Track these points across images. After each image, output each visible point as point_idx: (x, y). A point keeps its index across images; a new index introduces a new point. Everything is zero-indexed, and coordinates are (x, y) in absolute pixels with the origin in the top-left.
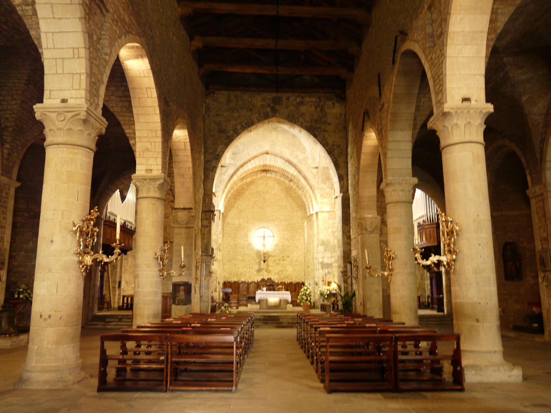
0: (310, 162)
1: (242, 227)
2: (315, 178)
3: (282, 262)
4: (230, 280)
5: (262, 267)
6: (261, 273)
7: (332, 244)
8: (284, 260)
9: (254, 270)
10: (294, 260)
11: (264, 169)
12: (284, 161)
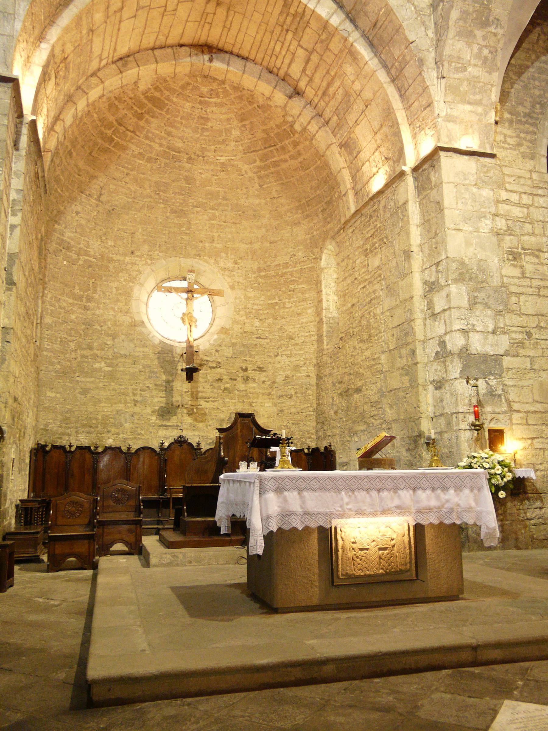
1: (111, 266)
2: (423, 23)
3: (241, 386)
4: (64, 442)
5: (177, 399)
6: (174, 421)
7: (496, 281)
8: (246, 379)
9: (149, 410)
10: (280, 379)
11: (203, 40)
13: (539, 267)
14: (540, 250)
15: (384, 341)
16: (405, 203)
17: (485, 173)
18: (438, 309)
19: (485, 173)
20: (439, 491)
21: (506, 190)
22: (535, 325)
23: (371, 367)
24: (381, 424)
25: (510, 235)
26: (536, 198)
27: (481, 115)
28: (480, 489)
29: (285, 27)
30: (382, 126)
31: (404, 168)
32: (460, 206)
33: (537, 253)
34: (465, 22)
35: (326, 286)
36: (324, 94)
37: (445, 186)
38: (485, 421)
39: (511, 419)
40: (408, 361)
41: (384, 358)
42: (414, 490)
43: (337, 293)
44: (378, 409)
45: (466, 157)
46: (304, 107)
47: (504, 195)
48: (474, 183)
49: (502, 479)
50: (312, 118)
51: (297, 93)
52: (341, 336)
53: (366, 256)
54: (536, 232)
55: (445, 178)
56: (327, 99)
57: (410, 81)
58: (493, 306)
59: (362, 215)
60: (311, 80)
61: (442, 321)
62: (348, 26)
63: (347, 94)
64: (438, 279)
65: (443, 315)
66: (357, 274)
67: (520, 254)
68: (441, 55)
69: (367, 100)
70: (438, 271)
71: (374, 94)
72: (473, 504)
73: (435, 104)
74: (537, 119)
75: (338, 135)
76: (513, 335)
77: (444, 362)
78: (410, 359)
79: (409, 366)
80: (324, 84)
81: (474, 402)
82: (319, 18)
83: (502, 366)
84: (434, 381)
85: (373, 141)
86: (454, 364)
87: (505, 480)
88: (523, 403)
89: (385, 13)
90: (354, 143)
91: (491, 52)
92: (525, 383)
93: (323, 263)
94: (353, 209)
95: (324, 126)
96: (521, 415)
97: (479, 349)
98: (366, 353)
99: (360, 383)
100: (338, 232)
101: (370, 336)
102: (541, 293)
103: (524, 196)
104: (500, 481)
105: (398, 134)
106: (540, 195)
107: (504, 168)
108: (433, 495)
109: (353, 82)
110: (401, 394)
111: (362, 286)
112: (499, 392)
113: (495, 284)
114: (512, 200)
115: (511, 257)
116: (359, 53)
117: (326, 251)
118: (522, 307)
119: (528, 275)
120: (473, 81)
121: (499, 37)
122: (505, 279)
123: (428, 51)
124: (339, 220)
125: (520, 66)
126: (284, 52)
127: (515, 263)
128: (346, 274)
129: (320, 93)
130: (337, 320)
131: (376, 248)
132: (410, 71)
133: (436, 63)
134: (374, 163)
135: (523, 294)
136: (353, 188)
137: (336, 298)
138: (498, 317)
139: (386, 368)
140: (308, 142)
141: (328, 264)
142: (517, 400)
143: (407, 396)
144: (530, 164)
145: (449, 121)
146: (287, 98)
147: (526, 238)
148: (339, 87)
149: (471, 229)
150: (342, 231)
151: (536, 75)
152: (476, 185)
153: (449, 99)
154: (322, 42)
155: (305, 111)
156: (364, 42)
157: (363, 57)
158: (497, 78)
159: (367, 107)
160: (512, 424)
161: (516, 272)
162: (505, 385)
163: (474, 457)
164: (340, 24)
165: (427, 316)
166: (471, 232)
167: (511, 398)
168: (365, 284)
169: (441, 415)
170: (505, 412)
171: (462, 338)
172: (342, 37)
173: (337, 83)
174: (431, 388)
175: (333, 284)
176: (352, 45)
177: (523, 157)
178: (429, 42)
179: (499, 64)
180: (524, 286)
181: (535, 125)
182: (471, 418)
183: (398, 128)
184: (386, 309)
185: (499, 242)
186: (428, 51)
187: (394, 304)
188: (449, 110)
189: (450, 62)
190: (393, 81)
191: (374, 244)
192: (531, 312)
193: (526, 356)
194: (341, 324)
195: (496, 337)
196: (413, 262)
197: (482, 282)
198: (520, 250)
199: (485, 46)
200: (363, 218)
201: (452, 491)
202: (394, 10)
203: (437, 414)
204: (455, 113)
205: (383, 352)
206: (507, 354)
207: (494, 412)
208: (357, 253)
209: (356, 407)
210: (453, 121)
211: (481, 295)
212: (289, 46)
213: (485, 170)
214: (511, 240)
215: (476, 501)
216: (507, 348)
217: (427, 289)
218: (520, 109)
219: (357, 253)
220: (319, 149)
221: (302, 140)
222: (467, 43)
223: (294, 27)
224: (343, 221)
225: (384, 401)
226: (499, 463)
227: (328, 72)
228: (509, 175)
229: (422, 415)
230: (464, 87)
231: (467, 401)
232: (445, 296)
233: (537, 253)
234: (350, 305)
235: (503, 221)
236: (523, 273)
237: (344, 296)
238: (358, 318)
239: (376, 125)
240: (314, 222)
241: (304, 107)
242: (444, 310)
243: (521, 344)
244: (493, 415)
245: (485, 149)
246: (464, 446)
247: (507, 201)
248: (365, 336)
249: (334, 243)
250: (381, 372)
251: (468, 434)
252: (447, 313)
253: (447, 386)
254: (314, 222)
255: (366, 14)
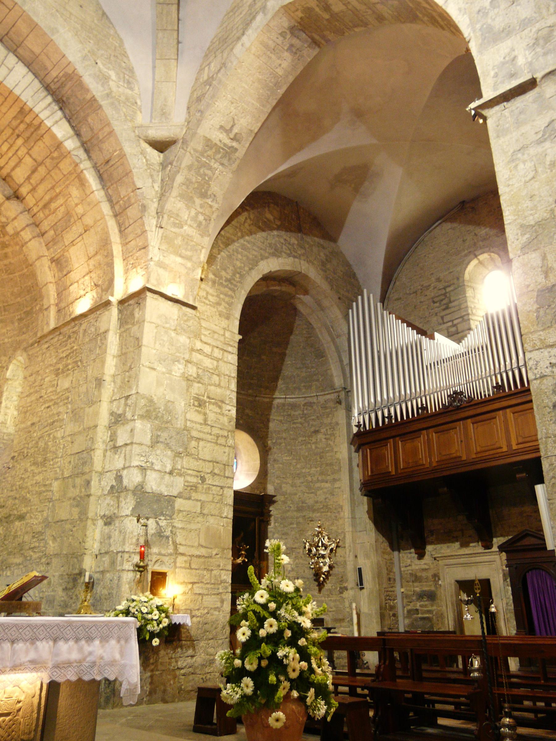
0: (141, 119)
7: (180, 424)
12: (37, 84)
13: (220, 417)
14: (222, 402)
15: (59, 467)
16: (106, 332)
17: (185, 321)
18: (120, 443)
19: (185, 321)
20: (83, 642)
21: (201, 340)
22: (209, 471)
23: (40, 493)
24: (40, 558)
25: (199, 382)
26: (225, 354)
27: (189, 269)
28: (127, 640)
29: (17, 132)
30: (96, 253)
31: (111, 298)
32: (157, 346)
33: (220, 404)
34: (188, 188)
35: (7, 398)
36: (45, 206)
37: (146, 324)
38: (150, 563)
39: (175, 562)
40: (81, 492)
41: (56, 485)
42: (55, 640)
43: (18, 409)
44: (39, 541)
45: (170, 303)
46: (21, 213)
47: (199, 345)
48: (173, 328)
49: (158, 625)
50: (27, 226)
51: (17, 196)
52: (13, 454)
53: (57, 375)
54: (222, 384)
55: (148, 317)
56: (47, 212)
57: (131, 221)
58: (173, 448)
59: (60, 334)
60: (34, 189)
61: (123, 455)
62: (82, 154)
63: (68, 214)
64: (125, 412)
65: (124, 449)
66: (43, 392)
67: (205, 402)
68: (163, 208)
69: (87, 226)
70: (126, 405)
71: (96, 222)
72: (117, 656)
73: (150, 248)
74: (236, 286)
75: (52, 250)
76: (189, 479)
77: (118, 498)
78: (83, 490)
79: (81, 497)
80: (47, 198)
81: (142, 541)
82: (54, 137)
83: (174, 508)
84: (104, 516)
85: (86, 265)
86: (128, 500)
87: (161, 626)
88: (189, 546)
89: (119, 155)
90: (66, 261)
91: (205, 219)
92: (193, 526)
93: (9, 374)
94: (52, 325)
95: (38, 236)
96: (185, 558)
97: (154, 488)
98: (37, 478)
99: (24, 510)
100: (32, 345)
101: (45, 460)
102: (219, 442)
103: (215, 349)
104: (156, 628)
105: (111, 265)
106: (230, 352)
107: (202, 321)
108: (76, 646)
109: (77, 205)
110: (68, 526)
111: (47, 405)
112: (168, 533)
113: (179, 426)
114: (205, 351)
115: (196, 403)
116: (87, 181)
117: (14, 361)
118: (200, 452)
119: (209, 423)
120: (187, 238)
121: (214, 209)
122: (188, 423)
123: (152, 201)
124: (36, 334)
125: (228, 239)
126: (10, 154)
127: (200, 409)
128: (32, 391)
129: (41, 204)
130: (12, 437)
131: (68, 370)
132: (132, 212)
133: (157, 213)
134: (82, 286)
135: (203, 440)
136: (57, 305)
137: (16, 413)
138: (177, 459)
139: (57, 496)
140: (18, 247)
141: (14, 376)
142: (184, 543)
143: (74, 529)
144: (224, 323)
145: (161, 267)
146: (4, 199)
147: (212, 388)
148: (62, 205)
149: (164, 370)
150: (36, 345)
151: (240, 250)
152: (175, 330)
153: (163, 247)
154: (53, 158)
155: (22, 217)
156: (94, 173)
157: (90, 186)
158: (207, 242)
159: (85, 231)
160: (176, 567)
161: (199, 418)
162: (173, 527)
163: (133, 601)
164: (74, 149)
165: (108, 448)
166: (163, 373)
167: (179, 540)
168: (51, 404)
169: (106, 553)
170: (171, 555)
171: (139, 475)
172: (74, 162)
173: (60, 201)
174: (100, 523)
175: (15, 398)
176: (82, 171)
177: (220, 315)
178: (154, 193)
179: (210, 232)
180: (204, 433)
181: (234, 291)
182: (136, 559)
183: (112, 260)
184: (67, 433)
185: (189, 387)
186: (152, 201)
187: (77, 429)
188: (161, 257)
189: (170, 217)
190: (116, 216)
191: (67, 365)
192: (208, 458)
193: (197, 500)
194: (15, 442)
195: (172, 478)
196: (103, 391)
197: (167, 422)
198: (205, 398)
199: (202, 213)
200: (61, 337)
201: (97, 642)
202: (128, 156)
203: (103, 551)
204: (167, 261)
205: (56, 479)
206: (180, 496)
207: (160, 554)
208: (47, 371)
209: (15, 537)
210: (164, 268)
211: (164, 435)
212: (17, 151)
213: (185, 318)
214: (199, 388)
215: (122, 653)
216: (181, 490)
217: (113, 421)
218: (223, 273)
219: (47, 371)
220: (29, 258)
221: (12, 243)
222: (186, 205)
223: (27, 134)
224: (39, 335)
225: (48, 532)
226: (157, 607)
227: (53, 188)
228: (205, 328)
229: (86, 551)
230: (178, 241)
231: (134, 540)
232: (129, 430)
233: (220, 404)
234: (29, 423)
235: (195, 369)
236: (205, 420)
237: (25, 413)
238: (37, 439)
239: (91, 251)
240: (8, 328)
241: (21, 213)
242: (126, 445)
243: (194, 488)
244: (158, 557)
245: (188, 299)
246: (125, 588)
247: (200, 351)
248: (40, 460)
249: (25, 355)
250: (50, 500)
251: (131, 575)
252: (129, 448)
253: (117, 522)
254: (8, 328)
255: (100, 150)
